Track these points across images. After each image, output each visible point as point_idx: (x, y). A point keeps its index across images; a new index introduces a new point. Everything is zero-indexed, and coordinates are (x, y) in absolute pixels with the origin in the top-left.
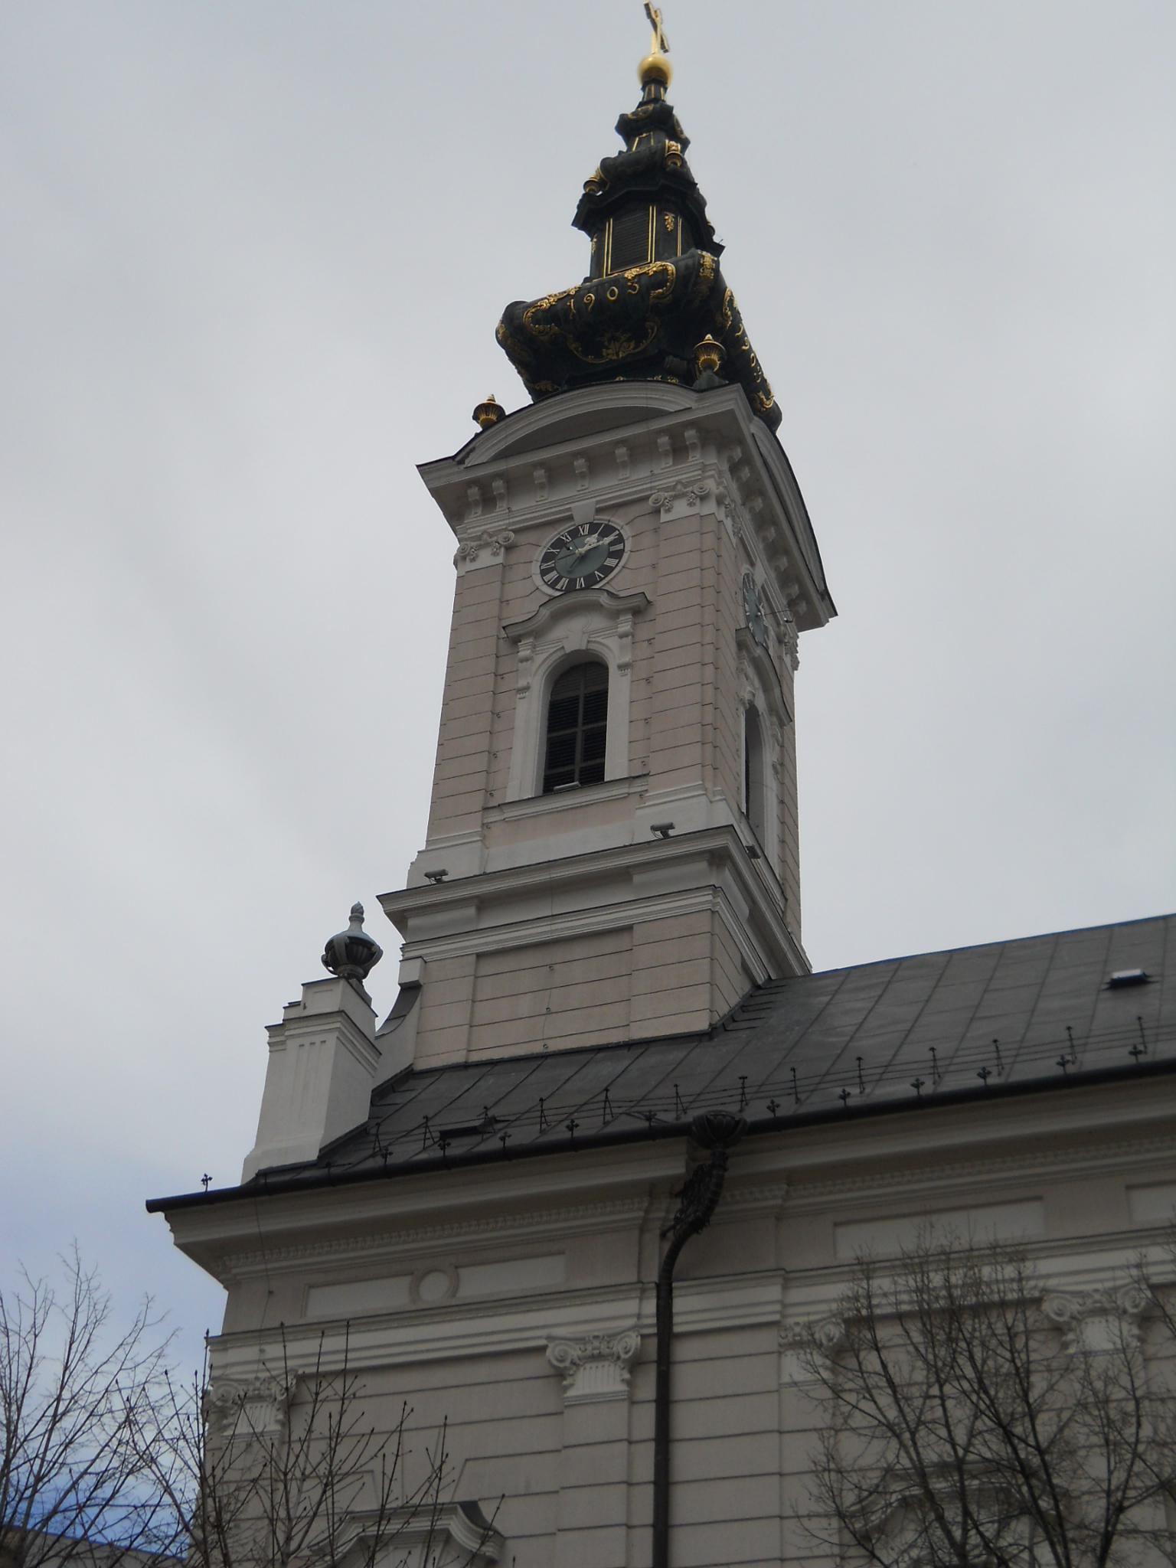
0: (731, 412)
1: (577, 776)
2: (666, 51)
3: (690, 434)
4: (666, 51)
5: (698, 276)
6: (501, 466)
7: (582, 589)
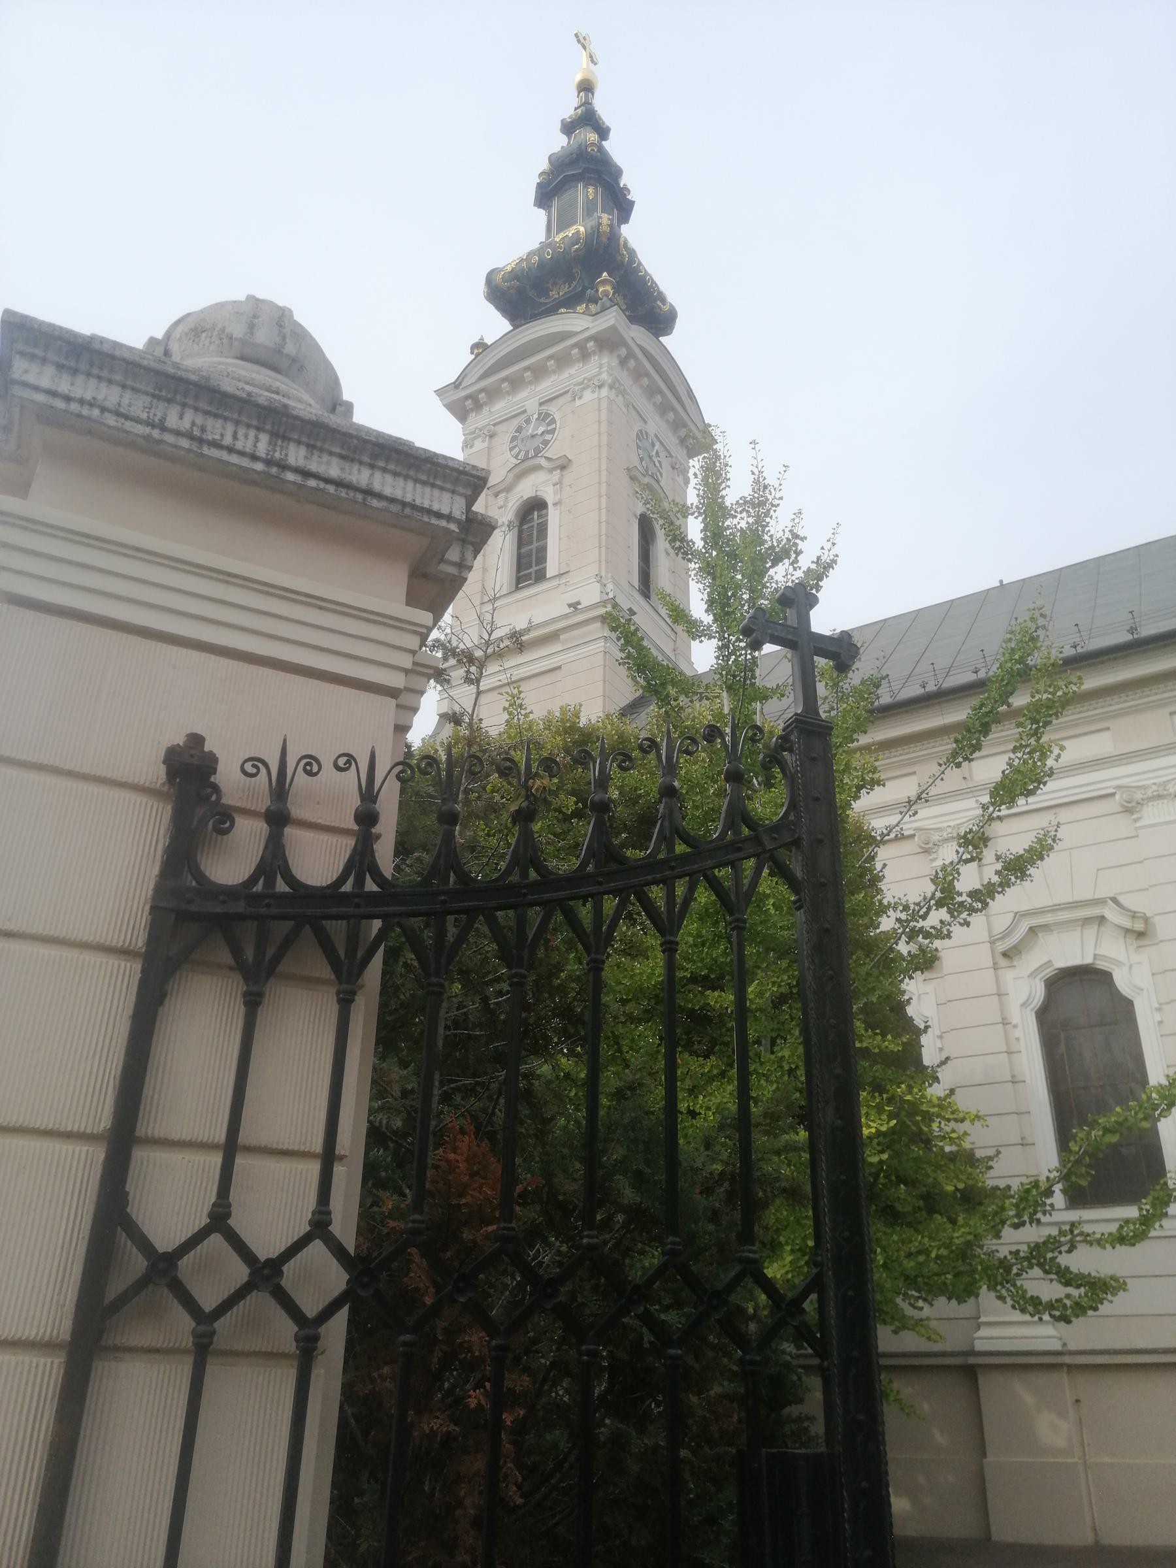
0: (613, 329)
1: (533, 577)
2: (595, 64)
3: (591, 344)
4: (595, 64)
5: (599, 232)
6: (482, 384)
7: (532, 457)
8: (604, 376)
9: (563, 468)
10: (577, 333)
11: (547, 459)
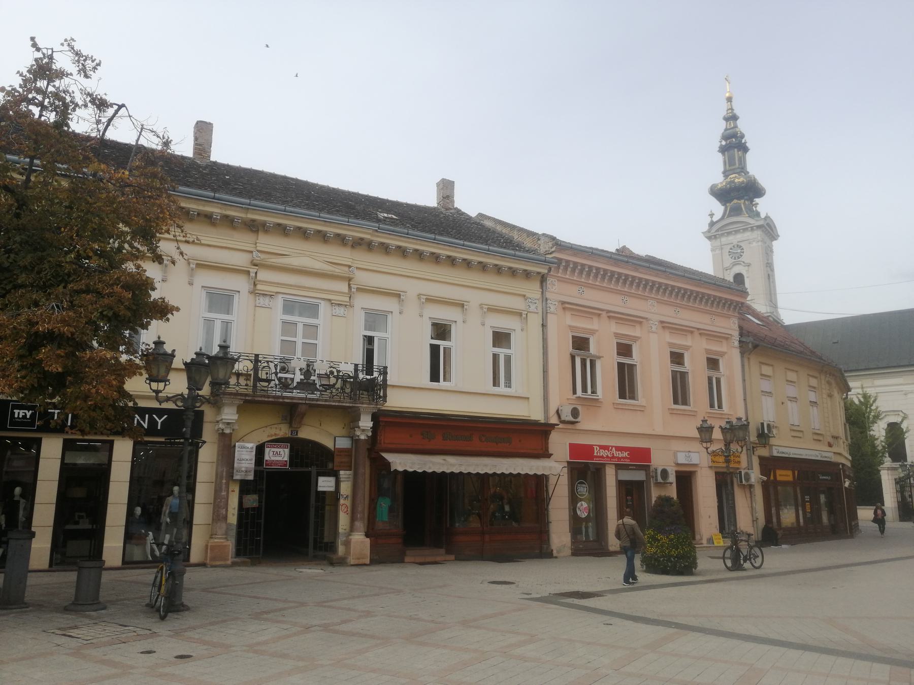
8: (759, 238)
9: (749, 266)
10: (751, 224)
11: (743, 262)
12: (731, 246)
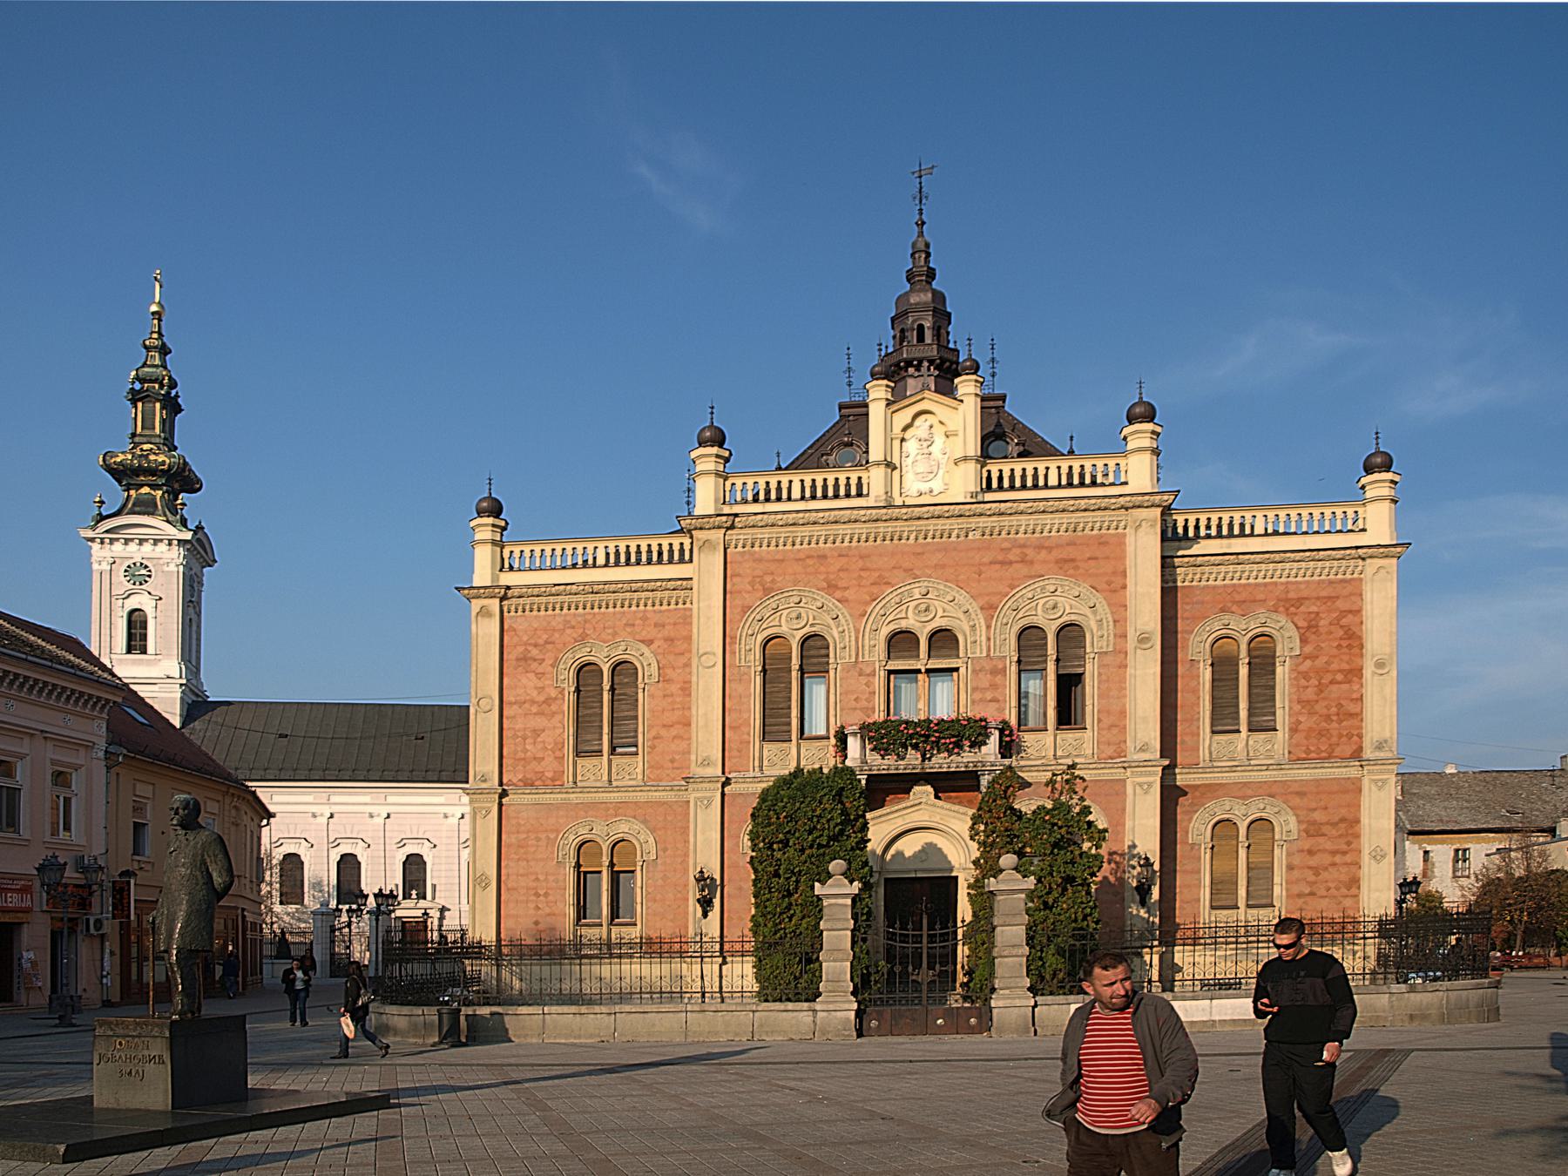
12: (130, 562)
